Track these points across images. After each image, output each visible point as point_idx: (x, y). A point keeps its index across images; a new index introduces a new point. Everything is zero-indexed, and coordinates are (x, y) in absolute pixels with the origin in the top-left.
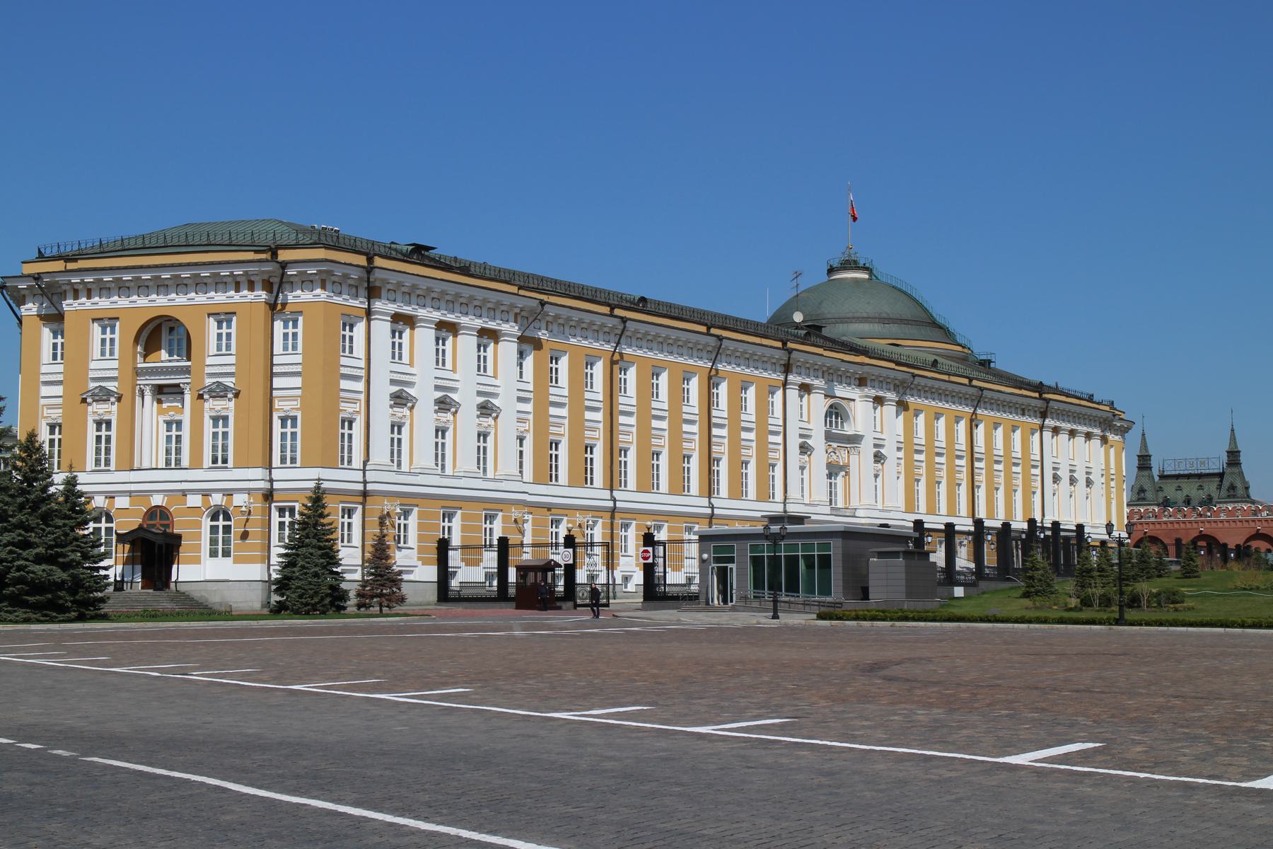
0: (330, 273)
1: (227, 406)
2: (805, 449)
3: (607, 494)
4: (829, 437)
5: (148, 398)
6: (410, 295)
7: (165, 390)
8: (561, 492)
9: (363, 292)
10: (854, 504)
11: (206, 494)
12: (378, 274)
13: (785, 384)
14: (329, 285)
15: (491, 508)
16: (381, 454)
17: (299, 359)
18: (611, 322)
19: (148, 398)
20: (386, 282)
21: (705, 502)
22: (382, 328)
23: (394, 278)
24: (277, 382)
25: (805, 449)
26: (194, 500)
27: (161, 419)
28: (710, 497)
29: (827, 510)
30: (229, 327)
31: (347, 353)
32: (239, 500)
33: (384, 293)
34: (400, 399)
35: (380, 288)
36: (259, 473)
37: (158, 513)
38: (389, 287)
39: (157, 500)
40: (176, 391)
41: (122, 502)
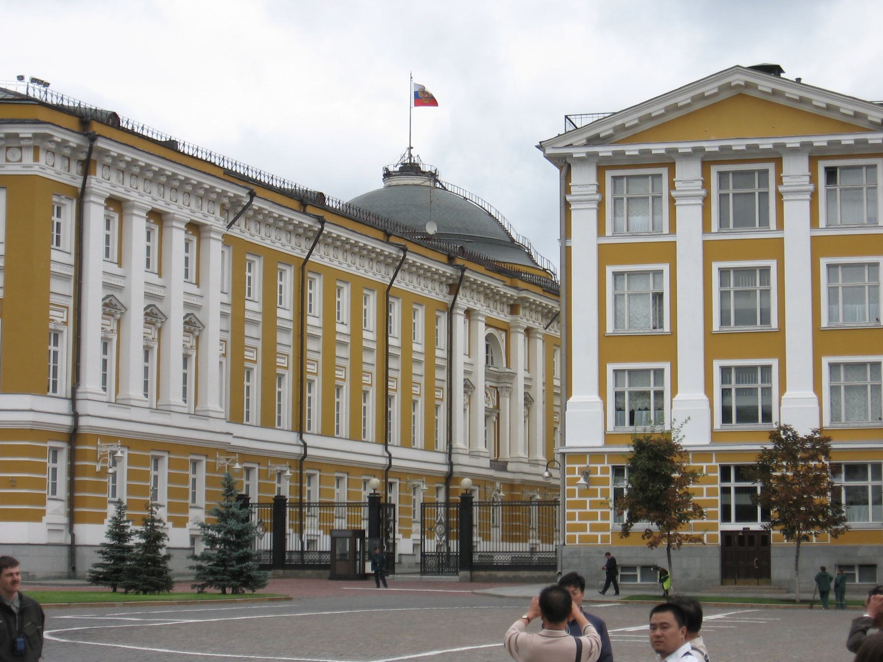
0: (47, 137)
2: (469, 387)
3: (293, 437)
4: (488, 375)
6: (128, 169)
8: (251, 435)
9: (76, 169)
10: (505, 455)
12: (101, 144)
13: (450, 310)
14: (43, 156)
15: (184, 452)
16: (91, 381)
18: (307, 222)
20: (104, 152)
21: (379, 449)
23: (115, 150)
25: (469, 387)
28: (386, 445)
29: (486, 463)
31: (54, 246)
34: (113, 308)
35: (95, 162)
38: (108, 160)
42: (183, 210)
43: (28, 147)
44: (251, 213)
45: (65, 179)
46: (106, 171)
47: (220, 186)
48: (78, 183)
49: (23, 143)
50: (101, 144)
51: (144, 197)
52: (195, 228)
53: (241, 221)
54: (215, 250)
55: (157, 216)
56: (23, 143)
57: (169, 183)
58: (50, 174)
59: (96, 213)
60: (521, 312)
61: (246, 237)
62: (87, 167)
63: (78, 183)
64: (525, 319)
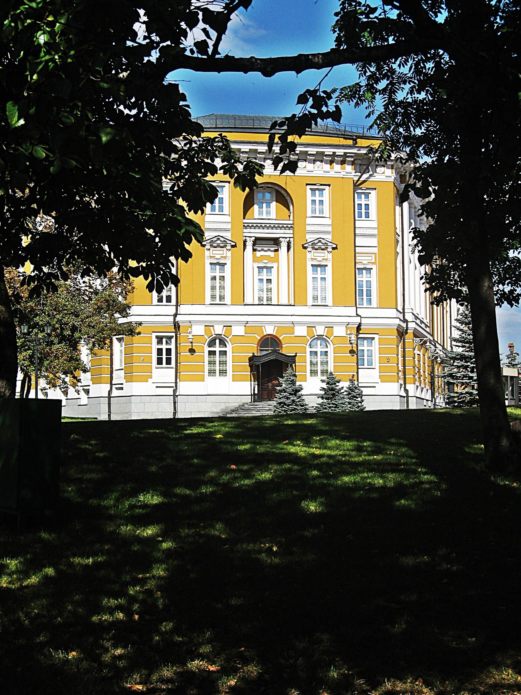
1: (326, 257)
5: (249, 247)
7: (257, 242)
11: (311, 327)
17: (375, 224)
19: (249, 247)
24: (359, 241)
26: (301, 331)
27: (256, 265)
30: (321, 195)
32: (340, 331)
36: (352, 311)
37: (270, 342)
39: (270, 330)
40: (276, 242)
41: (238, 330)
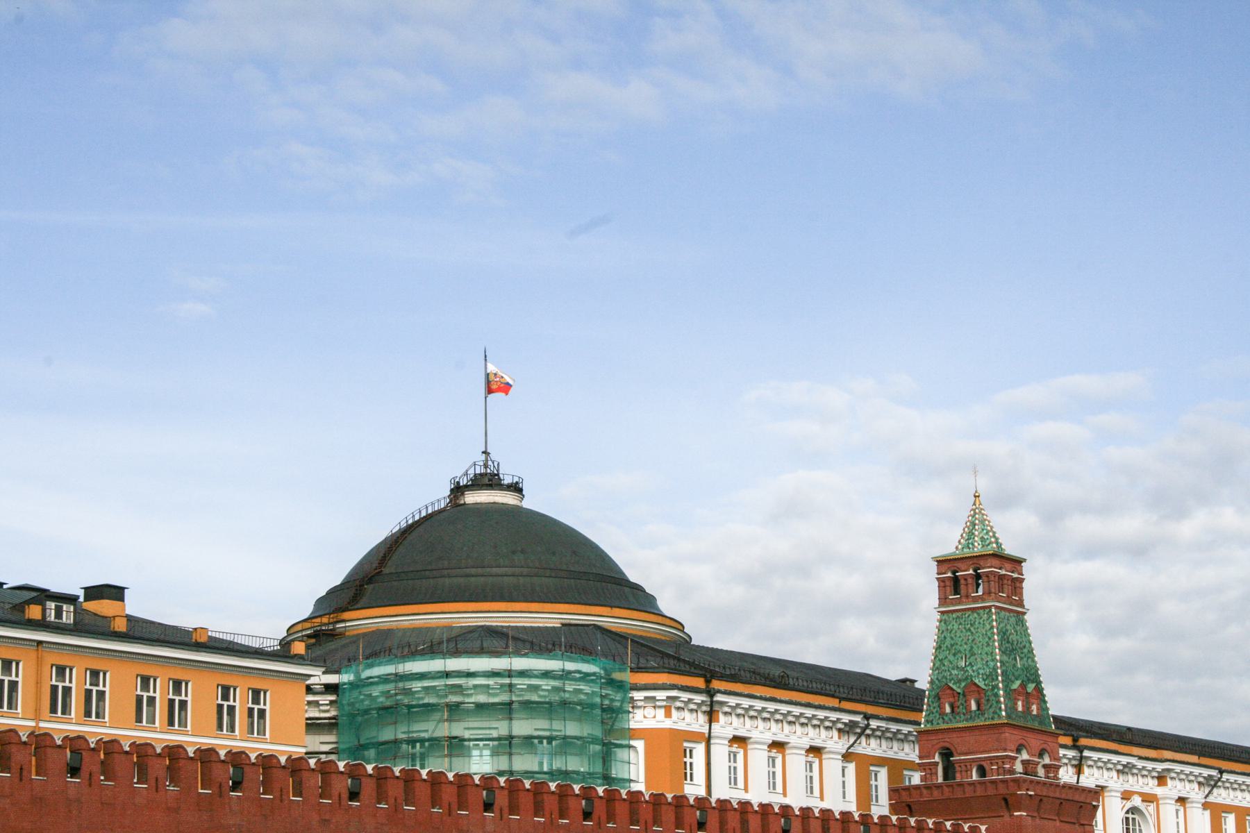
9: (702, 719)
14: (674, 713)
20: (722, 703)
22: (720, 751)
33: (721, 716)
38: (726, 709)
42: (799, 737)
43: (660, 707)
44: (868, 732)
45: (696, 728)
46: (728, 719)
47: (834, 716)
48: (705, 730)
49: (658, 703)
50: (719, 698)
51: (762, 732)
52: (815, 750)
53: (863, 739)
54: (833, 765)
55: (778, 746)
56: (658, 703)
57: (786, 719)
58: (682, 726)
59: (720, 751)
60: (1169, 781)
61: (869, 752)
62: (711, 716)
63: (705, 730)
64: (1175, 788)
